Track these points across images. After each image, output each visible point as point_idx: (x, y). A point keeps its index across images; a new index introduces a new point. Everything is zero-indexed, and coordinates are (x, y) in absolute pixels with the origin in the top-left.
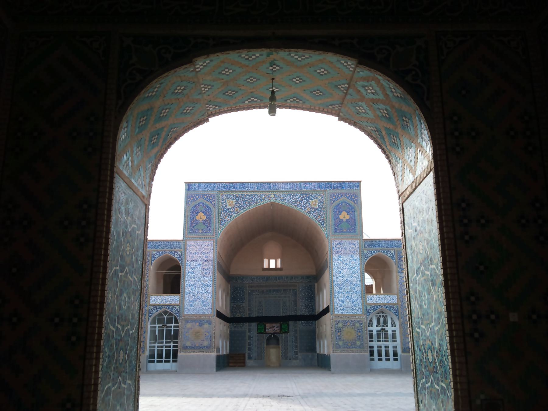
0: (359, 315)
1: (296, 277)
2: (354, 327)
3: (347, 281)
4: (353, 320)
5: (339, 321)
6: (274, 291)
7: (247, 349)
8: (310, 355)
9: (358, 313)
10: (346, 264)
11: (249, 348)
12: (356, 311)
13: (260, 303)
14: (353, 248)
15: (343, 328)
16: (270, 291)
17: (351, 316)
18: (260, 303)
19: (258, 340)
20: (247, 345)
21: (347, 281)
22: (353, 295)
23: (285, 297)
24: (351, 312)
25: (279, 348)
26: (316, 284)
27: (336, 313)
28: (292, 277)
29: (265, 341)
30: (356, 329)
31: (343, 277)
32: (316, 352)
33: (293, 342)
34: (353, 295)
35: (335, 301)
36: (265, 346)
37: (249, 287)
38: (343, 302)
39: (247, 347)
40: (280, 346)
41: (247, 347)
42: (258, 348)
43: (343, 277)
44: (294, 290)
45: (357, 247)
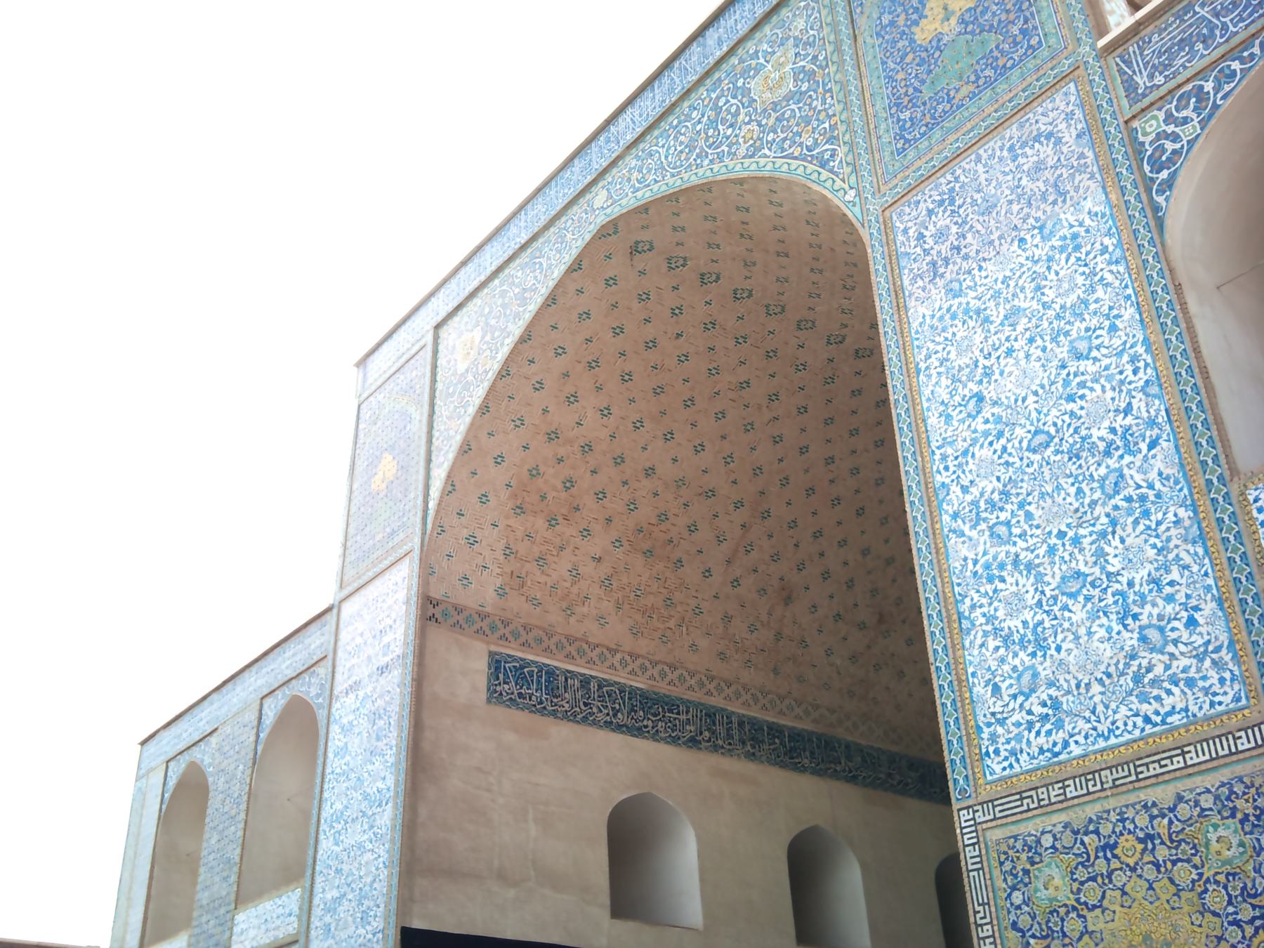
0: (1217, 730)
2: (1184, 874)
3: (1041, 440)
4: (1163, 795)
5: (1033, 848)
9: (1199, 706)
10: (1012, 316)
12: (1175, 699)
14: (1039, 167)
15: (1079, 908)
17: (1133, 764)
21: (1041, 440)
22: (1113, 547)
24: (1125, 721)
27: (996, 767)
30: (1215, 899)
31: (1002, 428)
34: (1113, 547)
35: (972, 656)
38: (1040, 645)
43: (1002, 428)
45: (1069, 137)
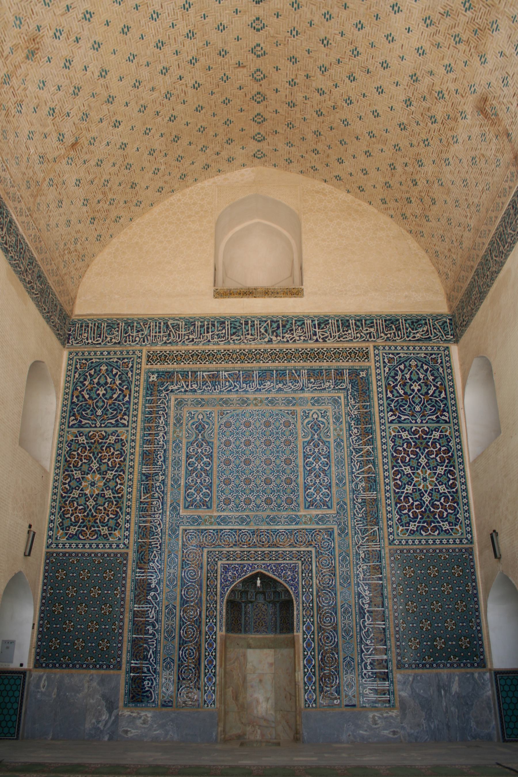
1: (363, 323)
6: (265, 375)
7: (126, 646)
8: (454, 678)
11: (134, 642)
13: (200, 428)
16: (248, 376)
18: (200, 428)
19: (184, 602)
20: (127, 625)
23: (317, 401)
25: (292, 643)
26: (454, 349)
28: (345, 323)
29: (221, 609)
32: (483, 664)
33: (362, 613)
36: (221, 632)
37: (150, 359)
39: (127, 636)
40: (299, 635)
41: (127, 636)
42: (182, 643)
44: (354, 373)
